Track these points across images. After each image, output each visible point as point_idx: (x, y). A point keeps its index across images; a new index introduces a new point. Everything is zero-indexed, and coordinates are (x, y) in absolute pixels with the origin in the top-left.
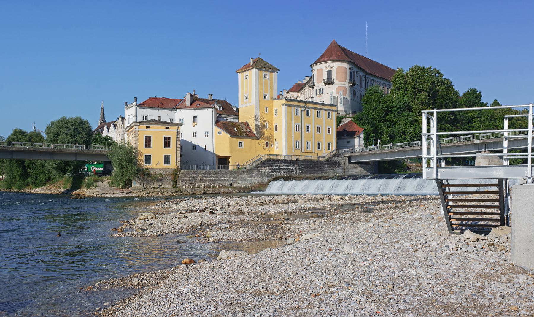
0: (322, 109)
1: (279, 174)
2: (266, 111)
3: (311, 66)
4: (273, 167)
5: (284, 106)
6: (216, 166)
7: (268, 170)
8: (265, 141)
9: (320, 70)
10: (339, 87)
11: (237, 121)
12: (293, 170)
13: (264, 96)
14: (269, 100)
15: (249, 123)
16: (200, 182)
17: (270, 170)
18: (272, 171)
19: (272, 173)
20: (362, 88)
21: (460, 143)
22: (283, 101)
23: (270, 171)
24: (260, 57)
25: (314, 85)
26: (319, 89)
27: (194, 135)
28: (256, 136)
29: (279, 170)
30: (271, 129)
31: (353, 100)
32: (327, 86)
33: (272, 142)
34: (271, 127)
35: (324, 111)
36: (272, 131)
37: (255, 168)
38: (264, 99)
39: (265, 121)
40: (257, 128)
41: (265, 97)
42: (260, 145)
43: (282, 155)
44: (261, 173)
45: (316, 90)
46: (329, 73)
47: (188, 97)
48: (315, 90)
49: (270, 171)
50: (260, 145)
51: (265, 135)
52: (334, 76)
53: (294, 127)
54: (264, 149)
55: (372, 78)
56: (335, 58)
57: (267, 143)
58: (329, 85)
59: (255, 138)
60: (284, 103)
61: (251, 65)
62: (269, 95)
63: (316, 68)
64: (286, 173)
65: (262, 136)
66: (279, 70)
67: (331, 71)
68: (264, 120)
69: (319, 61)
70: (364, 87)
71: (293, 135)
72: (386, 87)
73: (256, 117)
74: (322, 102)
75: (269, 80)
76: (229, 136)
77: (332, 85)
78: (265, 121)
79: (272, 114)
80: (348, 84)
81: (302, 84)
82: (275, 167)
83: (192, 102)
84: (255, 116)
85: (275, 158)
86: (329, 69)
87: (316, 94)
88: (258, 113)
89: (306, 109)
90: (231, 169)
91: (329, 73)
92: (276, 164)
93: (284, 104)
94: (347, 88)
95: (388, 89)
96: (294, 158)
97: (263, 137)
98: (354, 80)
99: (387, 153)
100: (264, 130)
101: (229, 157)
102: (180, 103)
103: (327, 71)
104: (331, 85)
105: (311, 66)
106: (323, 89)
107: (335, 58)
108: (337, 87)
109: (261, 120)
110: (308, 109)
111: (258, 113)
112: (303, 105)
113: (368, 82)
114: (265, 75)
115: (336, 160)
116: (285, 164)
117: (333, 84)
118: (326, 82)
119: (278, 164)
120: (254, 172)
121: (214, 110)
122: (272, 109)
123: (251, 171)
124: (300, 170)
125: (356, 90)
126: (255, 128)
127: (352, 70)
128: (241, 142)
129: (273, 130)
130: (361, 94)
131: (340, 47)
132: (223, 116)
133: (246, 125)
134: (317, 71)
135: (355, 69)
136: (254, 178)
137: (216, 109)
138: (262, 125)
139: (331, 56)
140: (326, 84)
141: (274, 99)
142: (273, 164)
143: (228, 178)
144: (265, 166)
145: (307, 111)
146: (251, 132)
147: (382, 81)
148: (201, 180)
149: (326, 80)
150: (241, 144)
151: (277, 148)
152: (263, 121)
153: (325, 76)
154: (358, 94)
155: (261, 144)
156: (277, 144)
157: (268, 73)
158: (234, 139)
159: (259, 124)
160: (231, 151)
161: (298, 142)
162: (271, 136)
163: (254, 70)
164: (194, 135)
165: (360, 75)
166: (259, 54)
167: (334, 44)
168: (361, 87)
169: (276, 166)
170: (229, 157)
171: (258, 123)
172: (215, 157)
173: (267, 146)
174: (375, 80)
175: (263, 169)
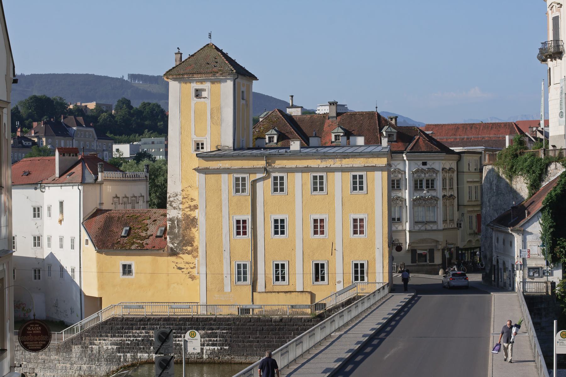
13: (198, 144)
17: (117, 344)
18: (122, 348)
19: (124, 352)
42: (180, 268)
44: (90, 352)
50: (180, 268)
65: (185, 245)
82: (134, 336)
92: (139, 329)
97: (189, 248)
119: (143, 329)
120: (73, 350)
124: (213, 345)
128: (127, 263)
136: (72, 364)
138: (187, 217)
142: (129, 329)
144: (101, 336)
145: (275, 178)
150: (127, 270)
152: (190, 207)
155: (182, 266)
157: (207, 86)
158: (108, 257)
159: (180, 216)
160: (101, 287)
161: (245, 266)
175: (97, 342)
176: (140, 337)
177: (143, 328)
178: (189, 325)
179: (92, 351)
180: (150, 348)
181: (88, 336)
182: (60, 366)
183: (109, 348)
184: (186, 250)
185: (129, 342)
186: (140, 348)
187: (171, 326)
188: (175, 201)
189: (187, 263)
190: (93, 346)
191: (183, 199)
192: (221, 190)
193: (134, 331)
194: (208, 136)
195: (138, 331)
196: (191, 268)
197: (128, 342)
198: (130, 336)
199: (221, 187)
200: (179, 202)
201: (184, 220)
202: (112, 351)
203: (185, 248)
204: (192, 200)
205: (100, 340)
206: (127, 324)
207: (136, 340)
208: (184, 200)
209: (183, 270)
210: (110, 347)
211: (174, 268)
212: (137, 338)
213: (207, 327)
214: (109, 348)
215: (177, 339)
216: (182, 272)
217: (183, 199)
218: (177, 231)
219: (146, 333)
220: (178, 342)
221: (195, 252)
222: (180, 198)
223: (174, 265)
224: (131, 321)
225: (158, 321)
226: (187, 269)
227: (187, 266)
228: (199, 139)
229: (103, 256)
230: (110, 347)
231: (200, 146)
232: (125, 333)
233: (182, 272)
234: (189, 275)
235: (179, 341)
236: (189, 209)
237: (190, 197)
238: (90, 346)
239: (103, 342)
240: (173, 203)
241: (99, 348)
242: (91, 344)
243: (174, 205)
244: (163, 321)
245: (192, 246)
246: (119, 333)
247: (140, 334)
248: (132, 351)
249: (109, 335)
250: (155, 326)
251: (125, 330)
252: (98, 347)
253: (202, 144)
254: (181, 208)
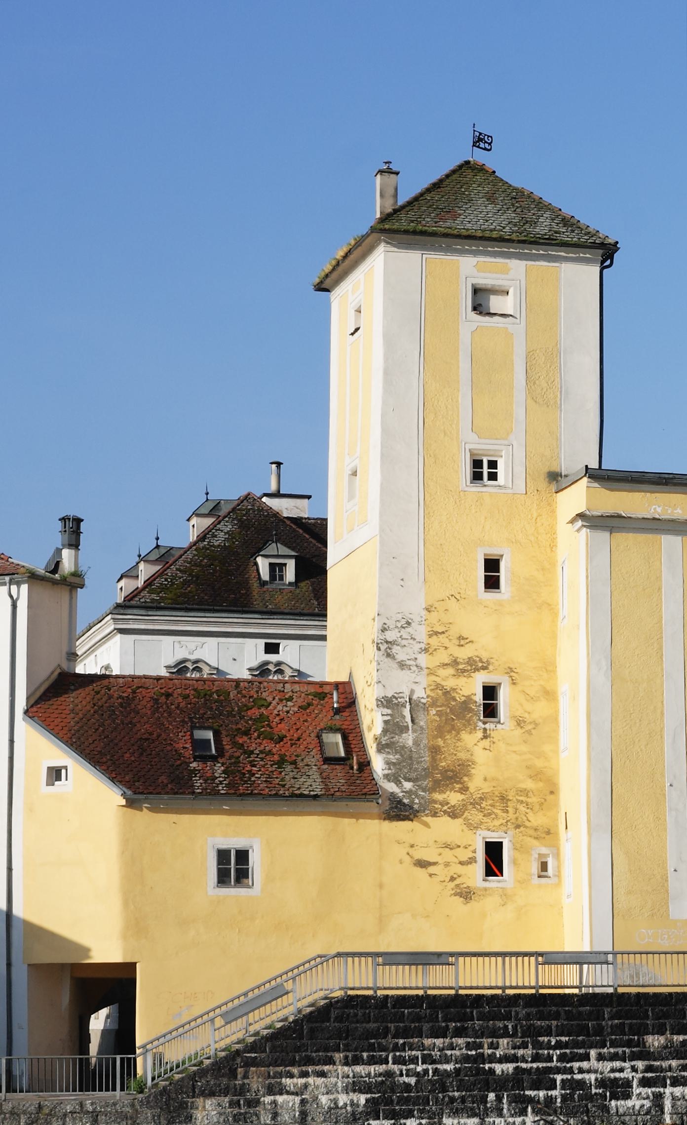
4: (398, 1061)
7: (357, 1086)
8: (473, 827)
12: (628, 1084)
13: (477, 464)
14: (520, 486)
23: (362, 1099)
24: (479, 157)
34: (539, 710)
36: (547, 748)
38: (476, 488)
42: (422, 864)
49: (362, 1099)
50: (422, 864)
54: (466, 894)
59: (372, 807)
60: (582, 509)
62: (520, 454)
68: (470, 661)
73: (390, 636)
75: (517, 329)
78: (475, 665)
84: (377, 626)
88: (415, 607)
93: (581, 516)
97: (454, 798)
111: (415, 607)
119: (459, 1033)
120: (199, 1115)
121: (24, 588)
128: (234, 843)
142: (406, 1033)
144: (309, 1061)
159: (420, 693)
162: (529, 784)
166: (480, 141)
172: (25, 968)
176: (448, 1062)
177: (456, 1028)
178: (612, 1018)
179: (275, 1115)
180: (484, 1100)
181: (253, 1063)
183: (341, 1104)
184: (445, 803)
185: (412, 1081)
186: (452, 1100)
187: (554, 1023)
188: (404, 642)
189: (447, 846)
190: (280, 1099)
191: (430, 636)
192: (660, 589)
193: (428, 1042)
194: (518, 439)
195: (439, 1042)
196: (461, 863)
197: (406, 1079)
198: (414, 1060)
199: (659, 578)
200: (417, 647)
201: (434, 704)
202: (353, 1114)
203: (438, 796)
204: (462, 641)
205: (305, 1075)
206: (401, 1018)
207: (436, 1071)
208: (434, 641)
209: (431, 869)
210: (343, 1099)
211: (401, 862)
212: (439, 1066)
213: (668, 1023)
214: (341, 1104)
215: (576, 1065)
216: (431, 875)
217: (430, 636)
218: (410, 743)
219: (468, 1046)
220: (578, 1077)
221: (474, 812)
222: (421, 632)
223: (401, 852)
224: (413, 1007)
225: (508, 1006)
226: (447, 865)
227: (448, 855)
228: (486, 448)
229: (145, 818)
230: (343, 1099)
231: (485, 470)
232: (396, 1048)
233: (431, 875)
234: (452, 885)
235: (581, 1071)
236: (451, 671)
237: (454, 632)
238: (268, 1099)
239: (320, 1081)
240: (395, 649)
241: (303, 1102)
242: (271, 1091)
243: (401, 654)
244: (525, 1007)
245: (464, 789)
246: (371, 1048)
247: (449, 1053)
248: (422, 1111)
249: (338, 1056)
250: (500, 1024)
251: (394, 1037)
252: (297, 1099)
253: (493, 464)
254: (424, 665)
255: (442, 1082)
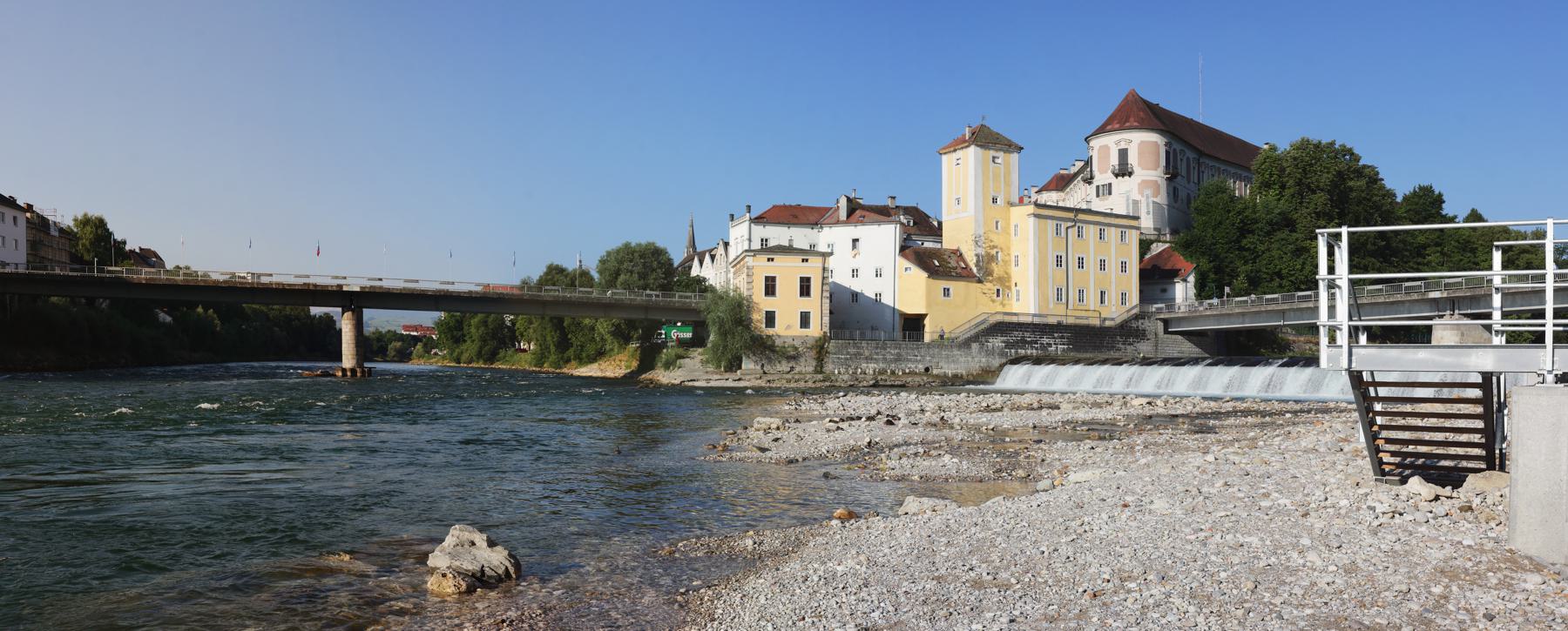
0: (1110, 225)
1: (1022, 352)
2: (997, 228)
3: (1087, 140)
5: (1032, 219)
6: (898, 334)
7: (1002, 342)
9: (1105, 149)
10: (1143, 181)
11: (939, 246)
15: (964, 250)
16: (867, 363)
17: (1004, 342)
18: (1009, 345)
20: (1192, 183)
21: (1399, 297)
22: (1031, 209)
24: (985, 123)
25: (1092, 178)
26: (1103, 186)
27: (855, 273)
28: (976, 276)
29: (1023, 343)
30: (1006, 263)
31: (1174, 207)
32: (1120, 178)
33: (1009, 288)
34: (1007, 258)
35: (1113, 229)
37: (975, 338)
39: (994, 247)
40: (978, 261)
41: (994, 200)
42: (985, 293)
43: (1028, 315)
45: (1098, 187)
46: (1123, 154)
47: (843, 203)
48: (1094, 186)
50: (985, 293)
51: (995, 275)
52: (1133, 159)
53: (1052, 261)
54: (993, 301)
55: (1211, 163)
56: (1136, 124)
57: (998, 290)
58: (1123, 177)
60: (1032, 212)
61: (967, 138)
63: (1096, 143)
64: (1037, 349)
65: (988, 275)
66: (1022, 148)
67: (1127, 149)
69: (1102, 130)
70: (1196, 181)
71: (1049, 270)
72: (1241, 181)
74: (1109, 211)
75: (1002, 167)
76: (925, 275)
77: (1130, 176)
78: (994, 247)
79: (1009, 234)
80: (1163, 175)
81: (1068, 175)
83: (850, 213)
85: (1014, 319)
86: (1123, 146)
87: (1098, 196)
89: (1078, 224)
90: (927, 338)
91: (1123, 154)
94: (1159, 182)
95: (1246, 186)
96: (1052, 320)
97: (991, 278)
98: (1175, 167)
99: (1243, 314)
100: (993, 264)
101: (925, 315)
102: (829, 214)
103: (1120, 150)
104: (1126, 178)
105: (1086, 140)
106: (1110, 185)
107: (1136, 124)
108: (1140, 181)
109: (987, 245)
110: (1080, 225)
111: (982, 233)
112: (1071, 215)
113: (1203, 172)
114: (994, 158)
115: (1137, 327)
116: (1034, 332)
117: (1130, 174)
118: (1117, 172)
122: (1009, 224)
123: (967, 344)
124: (1064, 344)
125: (1177, 186)
126: (975, 261)
127: (1170, 147)
129: (1010, 265)
130: (1188, 194)
131: (1146, 102)
132: (914, 238)
133: (958, 254)
134: (1099, 150)
135: (1177, 146)
136: (973, 358)
137: (902, 224)
138: (988, 254)
139: (1127, 121)
140: (1117, 176)
141: (1011, 205)
143: (921, 356)
145: (1079, 227)
146: (967, 267)
147: (1233, 170)
148: (869, 359)
149: (1117, 167)
150: (946, 292)
151: (1018, 300)
153: (1114, 160)
154: (1182, 194)
155: (985, 292)
156: (1018, 292)
157: (1001, 154)
160: (929, 305)
163: (973, 148)
164: (855, 273)
165: (1188, 158)
166: (983, 118)
167: (1133, 96)
168: (1189, 182)
169: (1017, 335)
170: (925, 315)
171: (981, 251)
173: (998, 295)
174: (1219, 168)
182: (962, 359)
194: (1002, 193)
204: (992, 241)
222: (983, 238)
223: (980, 290)
229: (931, 280)
255: (1017, 342)
